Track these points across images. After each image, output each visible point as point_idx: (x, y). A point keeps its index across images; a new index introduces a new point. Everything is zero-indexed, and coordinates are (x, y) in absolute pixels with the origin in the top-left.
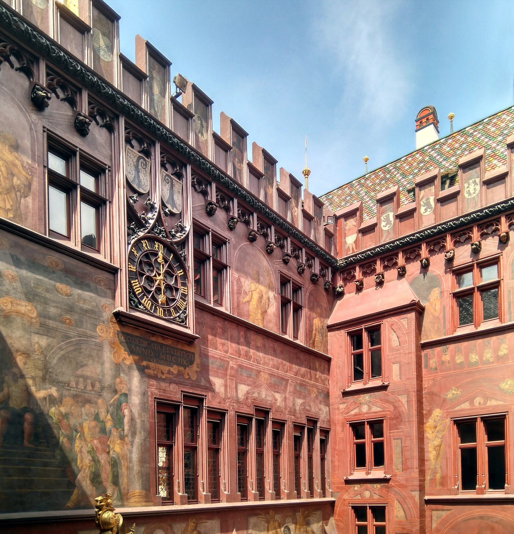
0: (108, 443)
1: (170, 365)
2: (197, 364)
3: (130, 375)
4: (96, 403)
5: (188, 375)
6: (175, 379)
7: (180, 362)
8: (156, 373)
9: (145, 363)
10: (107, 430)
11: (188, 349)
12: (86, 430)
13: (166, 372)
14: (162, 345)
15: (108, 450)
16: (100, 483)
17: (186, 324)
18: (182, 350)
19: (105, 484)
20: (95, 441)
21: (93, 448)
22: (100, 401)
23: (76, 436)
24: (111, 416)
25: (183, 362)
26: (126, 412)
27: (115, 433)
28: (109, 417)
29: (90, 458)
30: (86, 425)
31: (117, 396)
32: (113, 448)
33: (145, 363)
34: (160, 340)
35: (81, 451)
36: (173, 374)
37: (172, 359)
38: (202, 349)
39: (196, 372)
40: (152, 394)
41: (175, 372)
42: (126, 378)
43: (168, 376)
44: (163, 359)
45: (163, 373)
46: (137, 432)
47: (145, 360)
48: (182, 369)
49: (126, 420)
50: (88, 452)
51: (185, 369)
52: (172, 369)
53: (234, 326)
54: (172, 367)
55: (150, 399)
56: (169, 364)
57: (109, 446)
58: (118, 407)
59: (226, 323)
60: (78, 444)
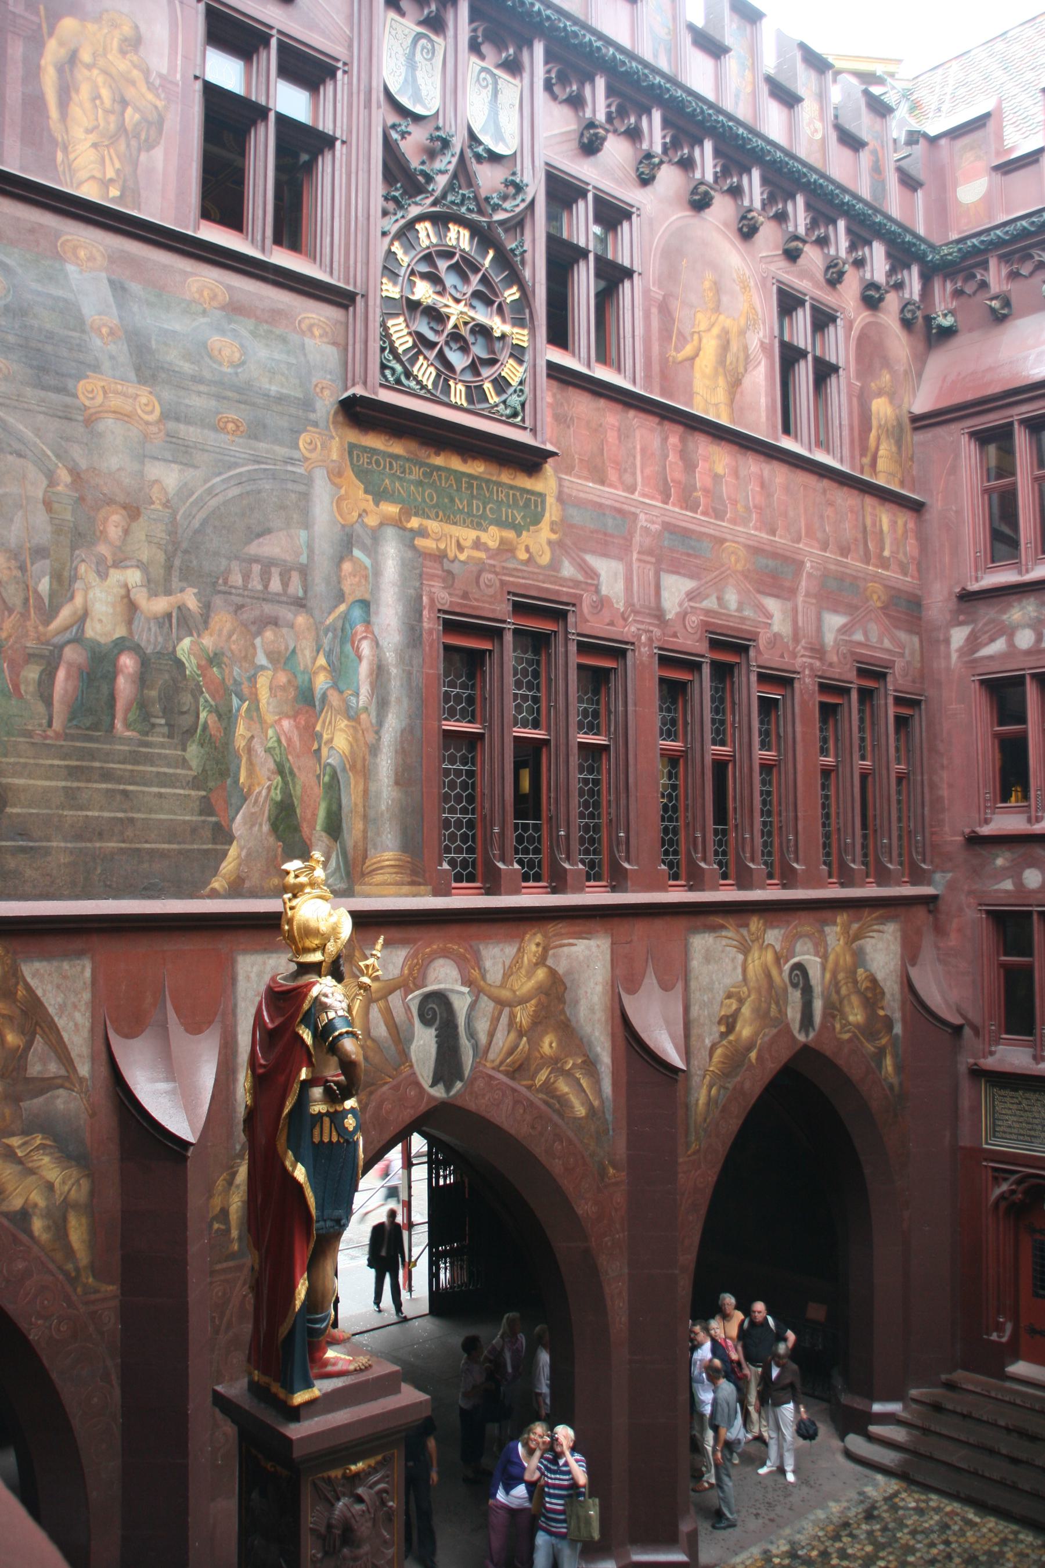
0: (318, 728)
1: (479, 526)
2: (552, 523)
3: (376, 552)
4: (292, 626)
6: (492, 562)
7: (507, 516)
8: (442, 546)
9: (414, 523)
10: (318, 695)
11: (524, 482)
12: (264, 695)
13: (468, 543)
14: (459, 475)
15: (316, 747)
16: (296, 829)
17: (523, 420)
18: (512, 487)
20: (286, 724)
21: (279, 741)
23: (239, 710)
24: (328, 657)
25: (514, 518)
26: (366, 648)
28: (322, 661)
29: (272, 765)
30: (263, 682)
31: (343, 607)
32: (331, 740)
33: (414, 523)
34: (456, 463)
35: (249, 750)
36: (487, 549)
37: (485, 508)
38: (566, 484)
39: (550, 543)
40: (432, 601)
41: (493, 544)
42: (367, 562)
44: (461, 511)
45: (460, 548)
46: (393, 699)
47: (416, 515)
48: (510, 534)
50: (268, 750)
51: (519, 535)
52: (485, 537)
53: (651, 421)
54: (485, 530)
55: (425, 613)
57: (318, 737)
58: (344, 634)
59: (632, 413)
60: (241, 729)
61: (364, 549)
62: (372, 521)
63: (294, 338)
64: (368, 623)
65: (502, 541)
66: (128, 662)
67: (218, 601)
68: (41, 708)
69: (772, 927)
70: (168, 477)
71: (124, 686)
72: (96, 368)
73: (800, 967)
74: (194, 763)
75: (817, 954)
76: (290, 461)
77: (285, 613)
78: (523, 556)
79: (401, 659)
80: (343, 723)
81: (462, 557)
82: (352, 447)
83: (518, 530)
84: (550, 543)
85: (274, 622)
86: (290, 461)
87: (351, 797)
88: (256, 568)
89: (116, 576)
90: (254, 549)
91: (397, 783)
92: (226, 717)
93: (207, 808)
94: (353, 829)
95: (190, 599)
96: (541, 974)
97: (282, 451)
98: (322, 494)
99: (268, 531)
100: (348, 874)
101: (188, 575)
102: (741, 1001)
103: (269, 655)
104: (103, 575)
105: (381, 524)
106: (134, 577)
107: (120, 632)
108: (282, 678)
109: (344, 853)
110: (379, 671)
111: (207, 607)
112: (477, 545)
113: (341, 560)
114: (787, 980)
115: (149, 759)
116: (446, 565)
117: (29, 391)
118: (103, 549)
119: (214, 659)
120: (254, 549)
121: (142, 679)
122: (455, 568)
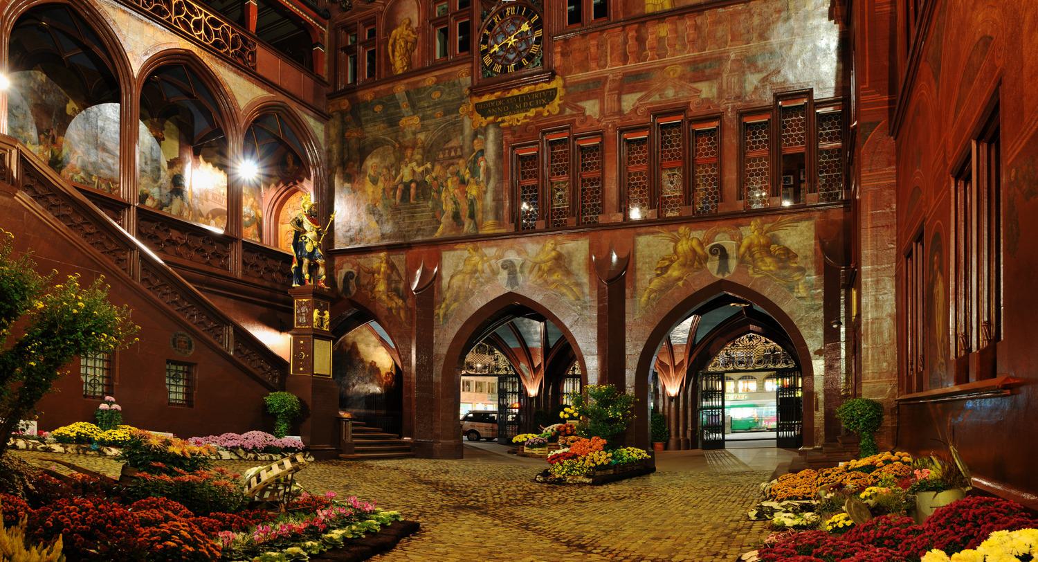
1: (527, 111)
5: (548, 111)
9: (500, 119)
19: (463, 218)
22: (461, 161)
26: (482, 164)
27: (472, 180)
28: (467, 171)
33: (500, 119)
35: (446, 200)
36: (529, 117)
42: (482, 137)
43: (525, 121)
45: (518, 121)
48: (540, 109)
49: (481, 170)
50: (451, 199)
52: (528, 114)
56: (527, 109)
57: (467, 192)
58: (475, 161)
60: (443, 195)
61: (482, 134)
62: (484, 125)
63: (457, 81)
64: (483, 155)
65: (536, 112)
66: (413, 185)
67: (436, 163)
68: (393, 200)
69: (695, 230)
70: (421, 137)
71: (413, 191)
72: (403, 116)
73: (718, 246)
74: (431, 206)
75: (732, 238)
76: (457, 117)
77: (456, 161)
78: (546, 114)
79: (496, 164)
80: (475, 187)
81: (519, 124)
82: (476, 104)
83: (544, 106)
84: (559, 105)
85: (453, 164)
86: (457, 117)
87: (478, 206)
88: (447, 151)
89: (410, 165)
90: (446, 147)
91: (494, 200)
92: (439, 193)
93: (434, 217)
94: (479, 216)
95: (429, 165)
96: (553, 254)
97: (454, 116)
98: (467, 122)
99: (451, 140)
100: (477, 228)
101: (428, 161)
102: (672, 262)
103: (452, 174)
104: (406, 166)
105: (488, 124)
106: (414, 164)
107: (411, 178)
108: (455, 179)
109: (475, 223)
110: (487, 170)
111: (433, 166)
112: (526, 117)
113: (473, 140)
114: (708, 253)
115: (419, 207)
116: (512, 129)
117: (389, 129)
118: (407, 160)
119: (435, 179)
120: (446, 147)
121: (417, 188)
122: (515, 129)
